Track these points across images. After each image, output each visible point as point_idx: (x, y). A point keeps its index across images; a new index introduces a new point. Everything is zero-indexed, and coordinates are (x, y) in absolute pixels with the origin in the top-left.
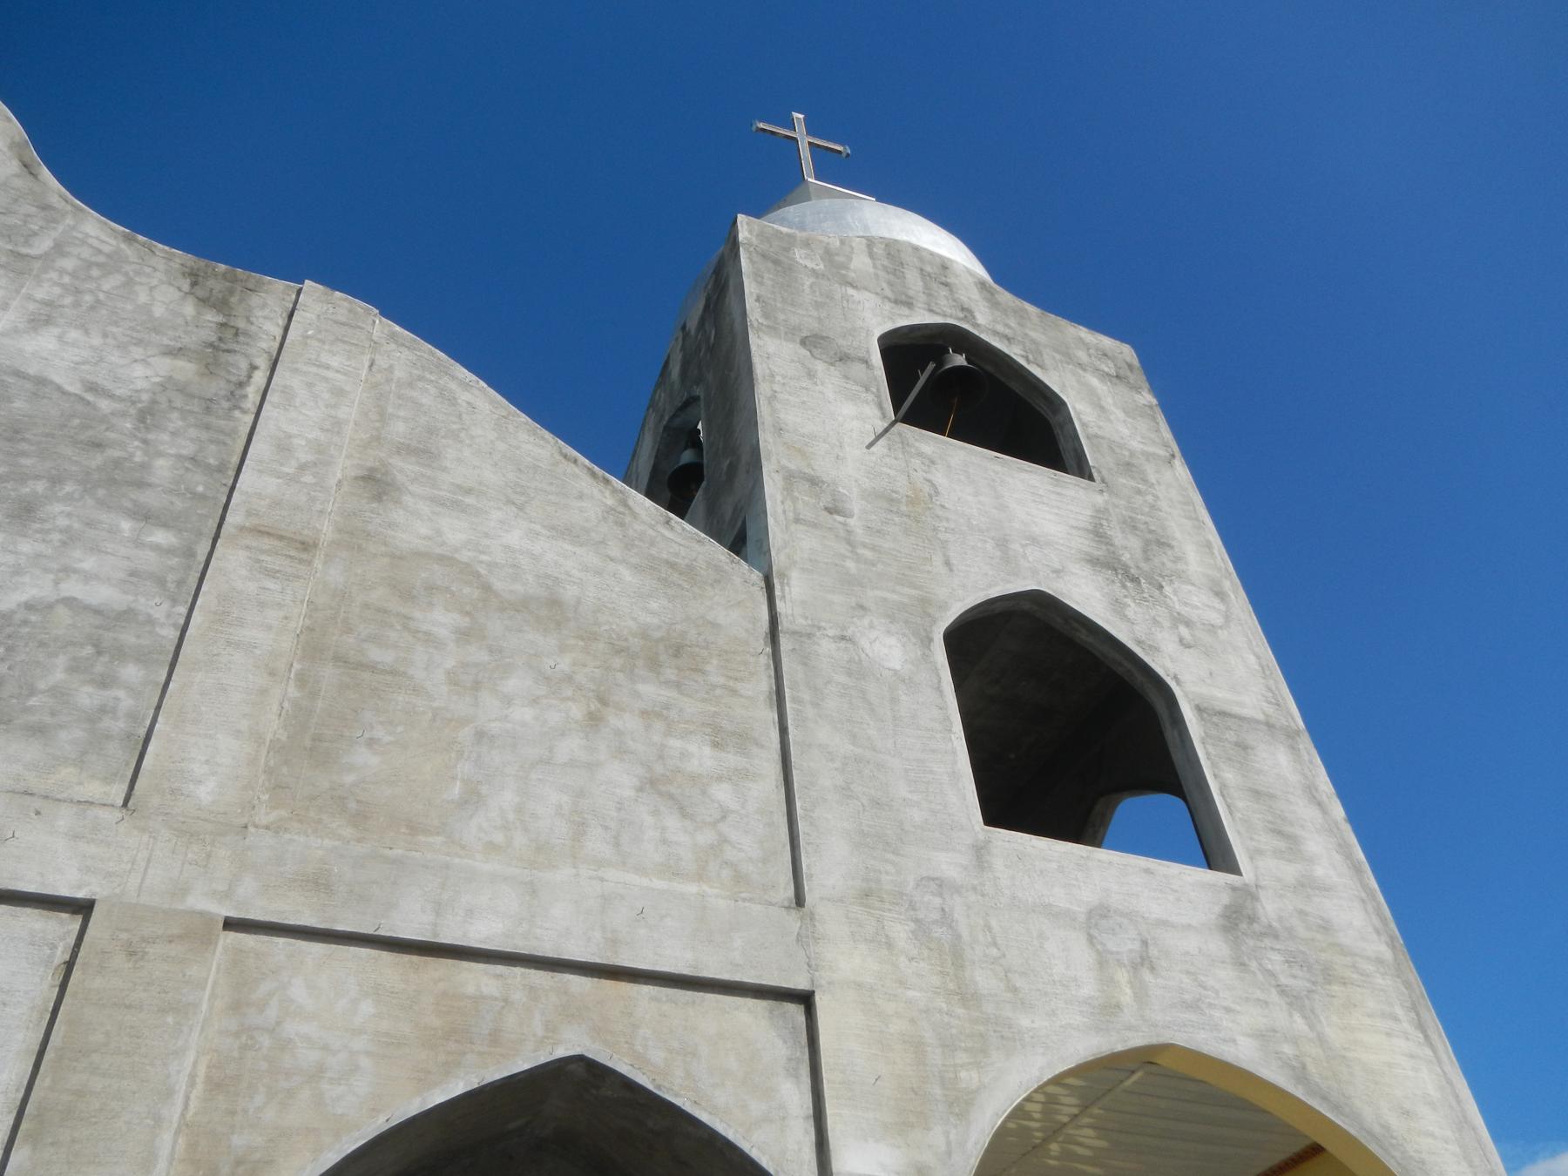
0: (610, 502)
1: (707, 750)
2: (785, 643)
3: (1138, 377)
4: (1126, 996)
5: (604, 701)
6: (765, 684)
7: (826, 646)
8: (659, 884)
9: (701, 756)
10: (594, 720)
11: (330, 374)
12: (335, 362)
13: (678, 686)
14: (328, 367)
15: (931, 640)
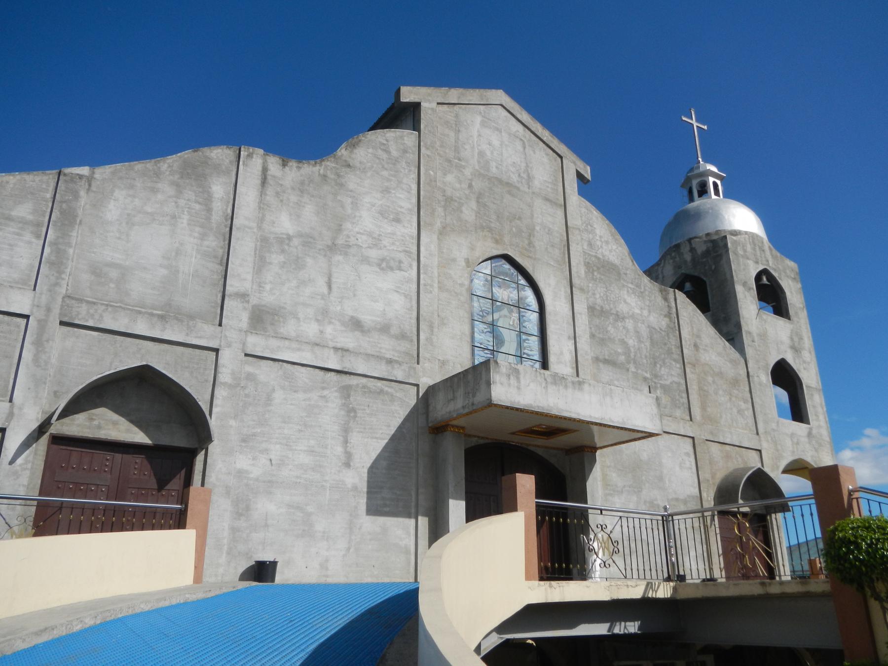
0: (723, 344)
1: (743, 404)
2: (750, 378)
3: (798, 277)
4: (795, 450)
5: (731, 394)
6: (747, 389)
7: (756, 378)
8: (742, 431)
9: (743, 406)
10: (730, 399)
11: (686, 319)
12: (685, 314)
13: (738, 390)
14: (684, 316)
15: (768, 375)
